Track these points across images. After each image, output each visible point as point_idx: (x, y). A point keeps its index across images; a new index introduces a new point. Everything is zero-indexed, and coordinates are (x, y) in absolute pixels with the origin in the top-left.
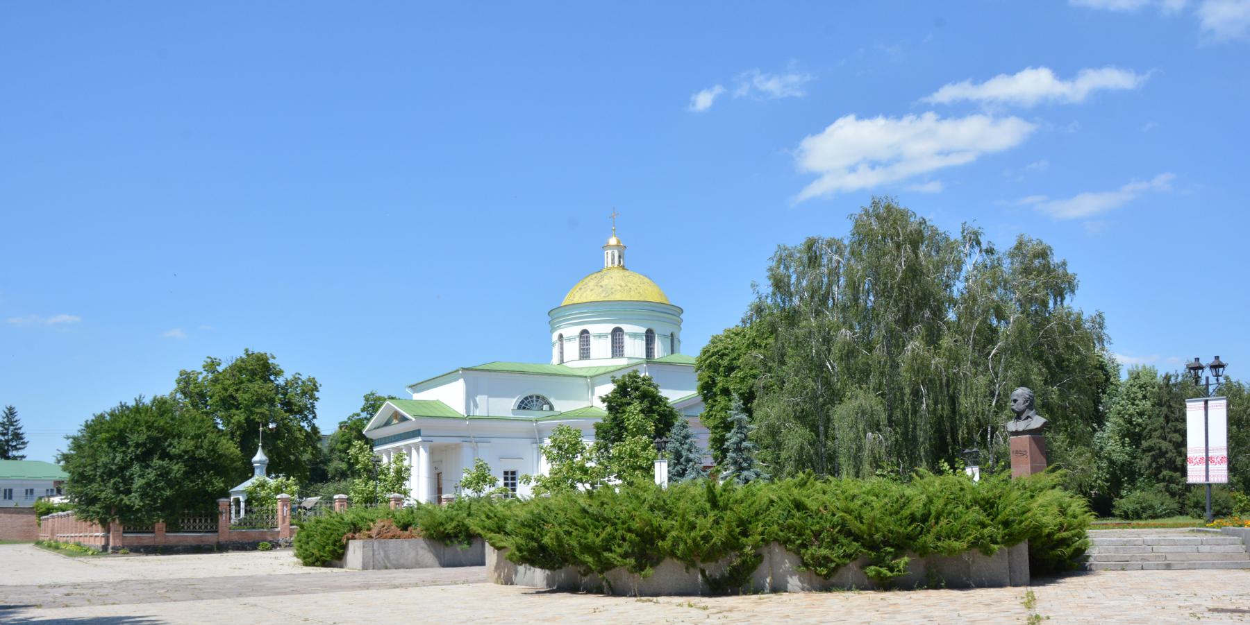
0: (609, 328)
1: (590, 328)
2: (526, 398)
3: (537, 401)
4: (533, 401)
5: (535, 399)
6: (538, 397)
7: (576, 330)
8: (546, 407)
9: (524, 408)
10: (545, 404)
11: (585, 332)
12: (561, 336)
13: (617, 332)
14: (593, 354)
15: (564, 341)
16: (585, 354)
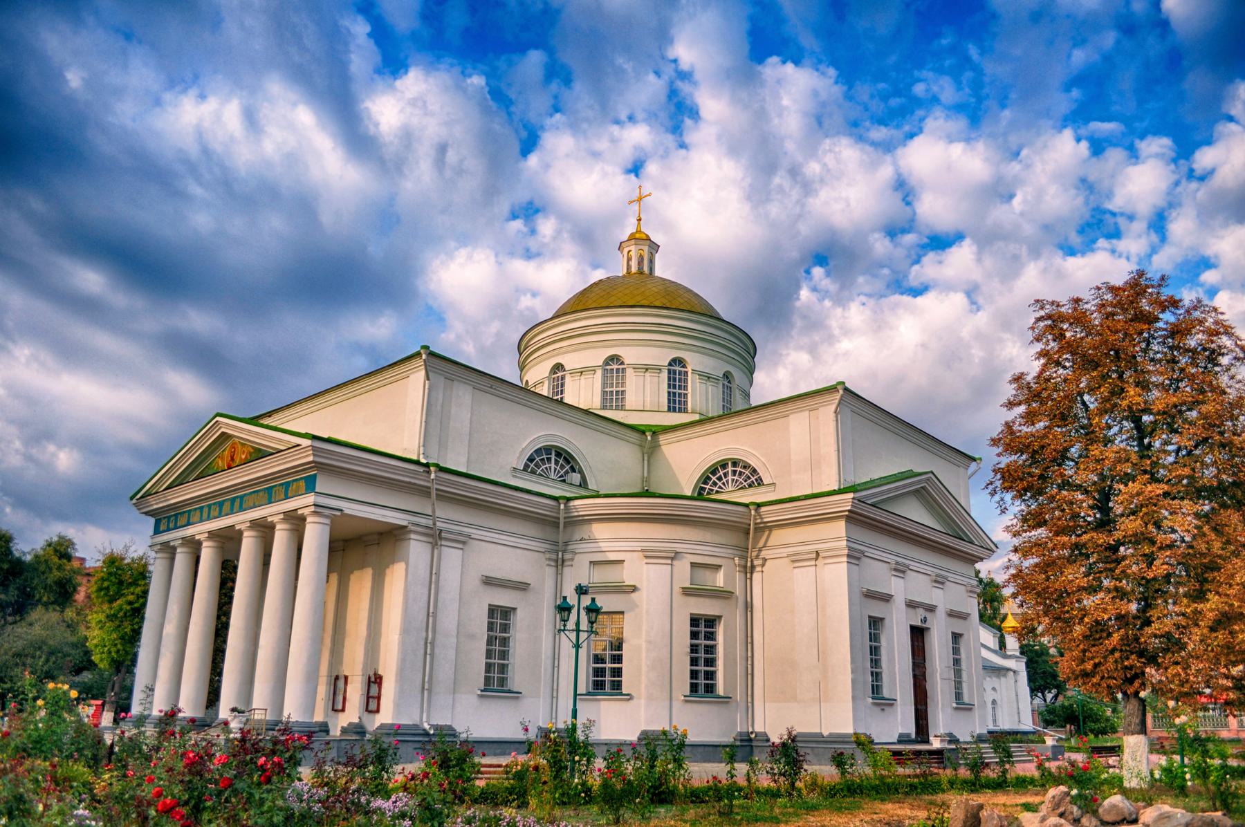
0: (662, 357)
1: (630, 355)
2: (538, 451)
3: (557, 463)
4: (549, 460)
5: (553, 457)
6: (560, 453)
7: (597, 357)
8: (576, 478)
9: (533, 472)
10: (573, 470)
11: (614, 359)
12: (558, 367)
13: (676, 371)
14: (631, 400)
15: (568, 379)
16: (613, 397)
